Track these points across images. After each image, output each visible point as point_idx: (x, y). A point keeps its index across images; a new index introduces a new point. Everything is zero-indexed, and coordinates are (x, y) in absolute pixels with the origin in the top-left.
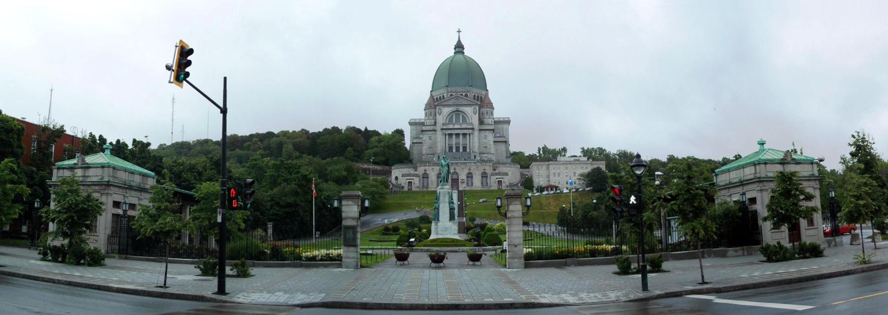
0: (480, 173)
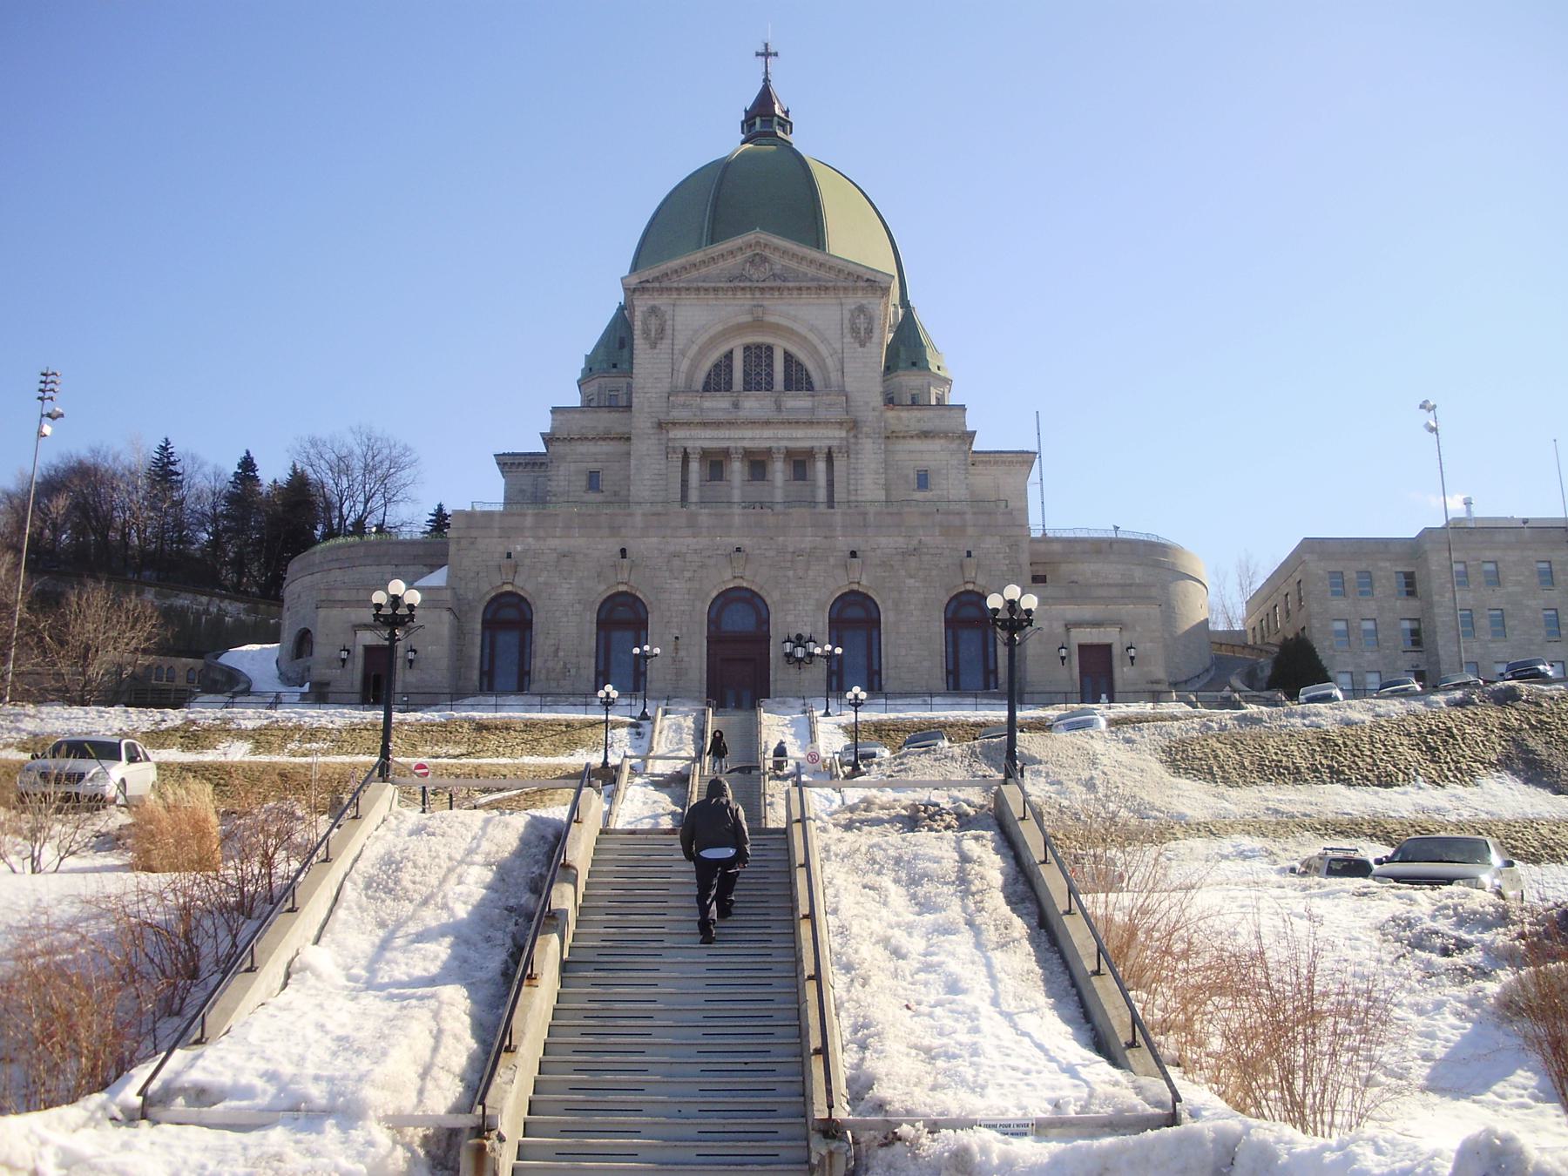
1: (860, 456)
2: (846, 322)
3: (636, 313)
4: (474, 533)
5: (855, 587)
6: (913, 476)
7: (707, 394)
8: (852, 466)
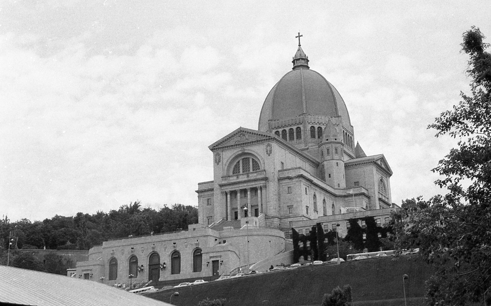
2: (265, 150)
6: (287, 189)
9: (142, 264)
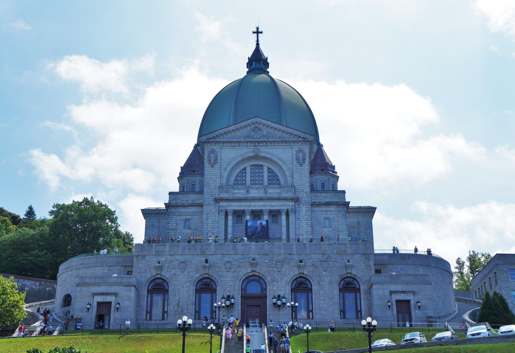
0: (338, 279)
1: (300, 213)
2: (294, 156)
3: (205, 152)
4: (144, 254)
5: (302, 275)
7: (235, 186)
8: (297, 217)
9: (228, 294)
